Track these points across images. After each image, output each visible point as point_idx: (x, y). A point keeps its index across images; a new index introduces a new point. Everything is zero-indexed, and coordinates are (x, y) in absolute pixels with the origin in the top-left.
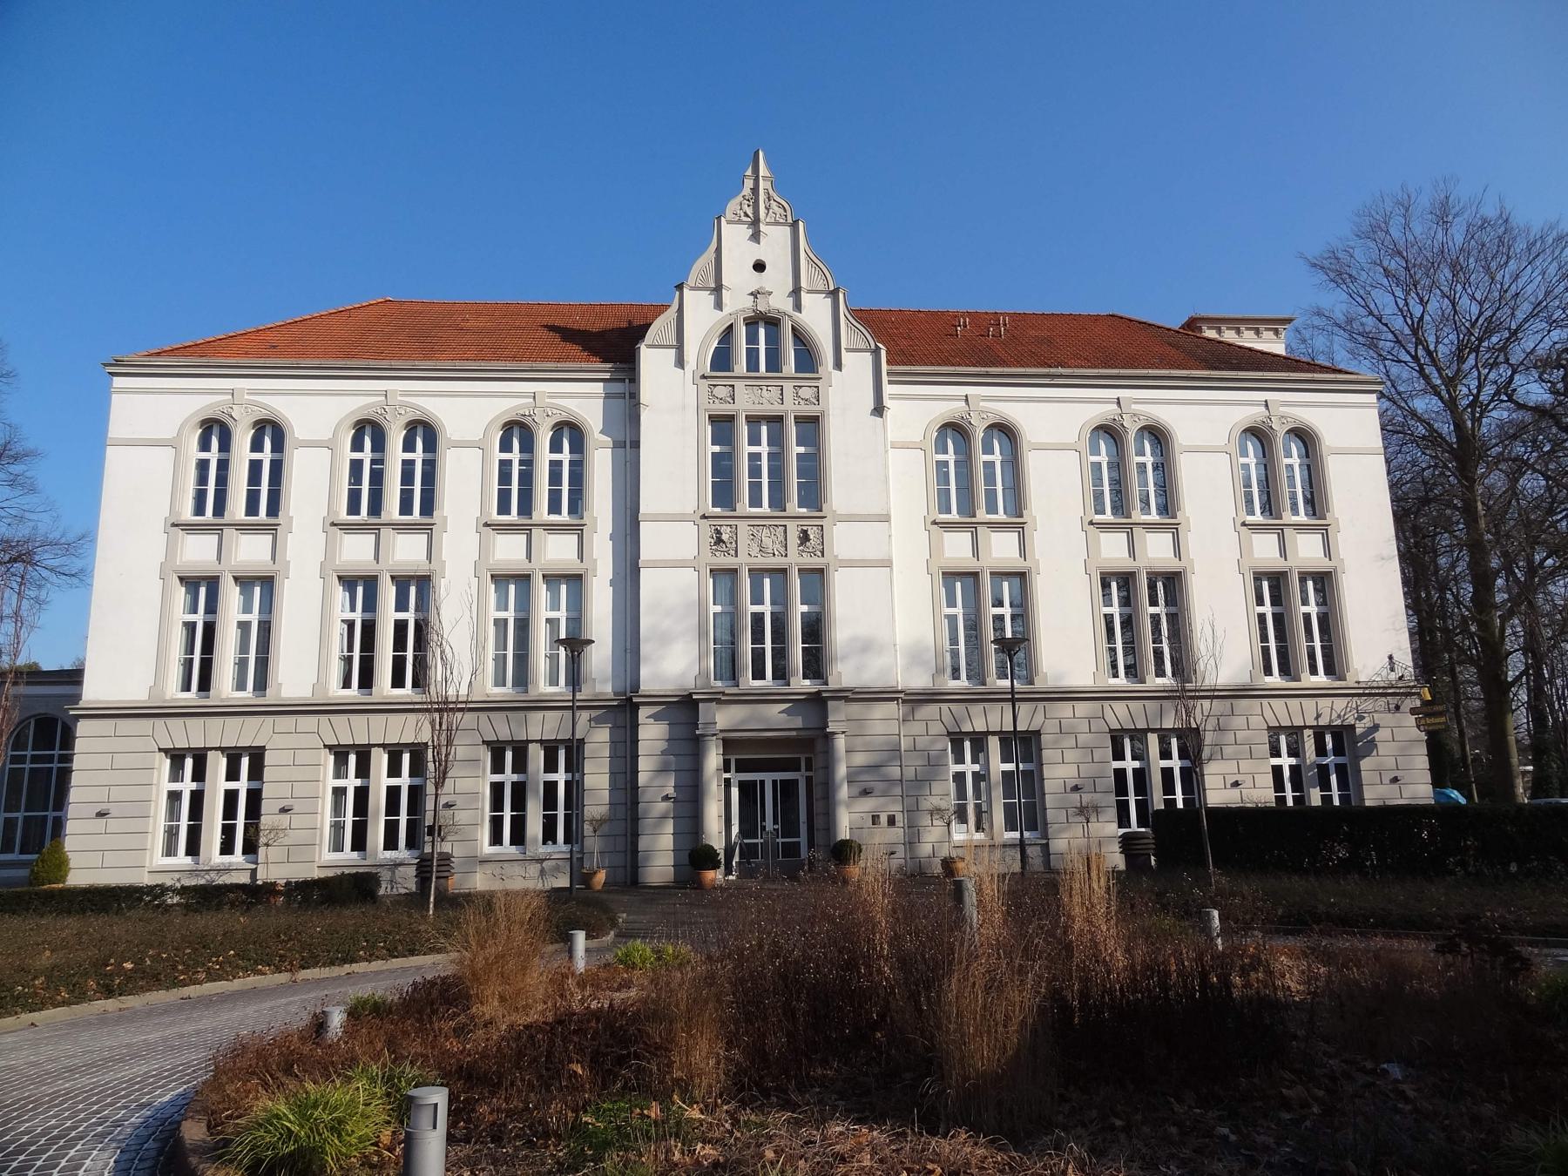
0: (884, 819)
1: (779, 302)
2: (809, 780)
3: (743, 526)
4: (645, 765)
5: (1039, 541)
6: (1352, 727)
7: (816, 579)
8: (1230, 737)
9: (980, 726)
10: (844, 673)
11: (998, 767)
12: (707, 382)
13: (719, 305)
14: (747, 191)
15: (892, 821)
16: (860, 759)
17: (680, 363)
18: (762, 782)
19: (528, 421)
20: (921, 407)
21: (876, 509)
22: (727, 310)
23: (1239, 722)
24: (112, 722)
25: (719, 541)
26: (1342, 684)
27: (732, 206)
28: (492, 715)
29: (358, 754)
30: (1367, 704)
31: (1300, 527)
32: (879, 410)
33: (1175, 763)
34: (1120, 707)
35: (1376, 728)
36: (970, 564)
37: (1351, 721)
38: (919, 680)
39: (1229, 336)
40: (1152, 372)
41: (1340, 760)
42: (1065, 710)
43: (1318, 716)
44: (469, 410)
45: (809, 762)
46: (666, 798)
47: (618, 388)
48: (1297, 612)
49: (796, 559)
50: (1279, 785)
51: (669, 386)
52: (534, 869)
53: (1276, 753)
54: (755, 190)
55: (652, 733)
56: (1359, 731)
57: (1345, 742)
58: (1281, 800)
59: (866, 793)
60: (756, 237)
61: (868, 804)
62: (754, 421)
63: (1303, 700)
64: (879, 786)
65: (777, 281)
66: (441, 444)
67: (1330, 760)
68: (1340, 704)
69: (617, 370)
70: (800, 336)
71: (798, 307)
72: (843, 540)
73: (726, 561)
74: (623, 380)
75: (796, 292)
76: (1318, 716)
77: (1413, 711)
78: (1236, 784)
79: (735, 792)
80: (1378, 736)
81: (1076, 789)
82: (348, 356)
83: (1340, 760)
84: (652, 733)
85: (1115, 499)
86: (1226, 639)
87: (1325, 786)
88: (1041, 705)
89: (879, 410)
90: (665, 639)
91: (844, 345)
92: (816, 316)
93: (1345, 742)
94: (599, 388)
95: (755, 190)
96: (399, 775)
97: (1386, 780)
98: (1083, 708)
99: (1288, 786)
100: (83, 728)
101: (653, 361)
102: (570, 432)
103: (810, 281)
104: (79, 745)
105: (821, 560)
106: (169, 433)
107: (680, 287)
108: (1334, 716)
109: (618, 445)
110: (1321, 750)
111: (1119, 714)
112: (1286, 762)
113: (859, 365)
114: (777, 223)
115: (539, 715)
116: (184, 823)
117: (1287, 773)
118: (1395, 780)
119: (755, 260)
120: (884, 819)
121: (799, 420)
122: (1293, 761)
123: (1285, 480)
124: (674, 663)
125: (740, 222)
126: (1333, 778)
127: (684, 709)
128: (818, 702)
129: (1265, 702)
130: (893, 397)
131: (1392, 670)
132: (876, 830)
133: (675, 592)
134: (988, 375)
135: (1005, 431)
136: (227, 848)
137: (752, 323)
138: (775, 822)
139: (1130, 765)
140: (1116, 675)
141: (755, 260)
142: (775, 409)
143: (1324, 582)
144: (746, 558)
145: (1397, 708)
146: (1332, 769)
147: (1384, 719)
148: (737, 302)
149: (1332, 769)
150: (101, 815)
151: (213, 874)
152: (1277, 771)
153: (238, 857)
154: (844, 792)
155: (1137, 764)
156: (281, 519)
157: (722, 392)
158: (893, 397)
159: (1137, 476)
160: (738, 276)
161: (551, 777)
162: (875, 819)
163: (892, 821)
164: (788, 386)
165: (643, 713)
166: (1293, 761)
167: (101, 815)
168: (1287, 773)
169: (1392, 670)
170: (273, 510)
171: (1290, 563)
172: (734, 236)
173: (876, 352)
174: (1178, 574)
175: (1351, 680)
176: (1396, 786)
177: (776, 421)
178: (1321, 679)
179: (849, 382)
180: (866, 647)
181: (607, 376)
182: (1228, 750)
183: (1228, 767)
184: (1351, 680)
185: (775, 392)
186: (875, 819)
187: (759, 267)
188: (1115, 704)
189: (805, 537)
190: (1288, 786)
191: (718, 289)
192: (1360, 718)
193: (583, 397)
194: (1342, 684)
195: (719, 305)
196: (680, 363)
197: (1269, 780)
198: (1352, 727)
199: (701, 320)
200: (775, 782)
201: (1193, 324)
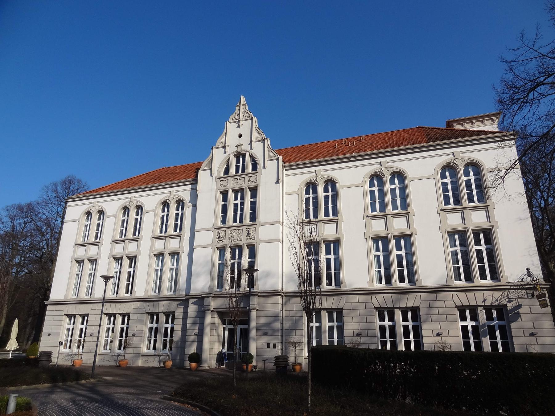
0: (272, 345)
1: (245, 147)
4: (189, 321)
5: (344, 226)
6: (506, 306)
7: (252, 249)
8: (435, 311)
10: (261, 285)
11: (326, 324)
13: (225, 153)
14: (237, 111)
16: (263, 320)
17: (211, 175)
19: (168, 201)
22: (228, 154)
23: (438, 304)
25: (219, 237)
26: (499, 284)
27: (232, 118)
30: (514, 294)
33: (410, 323)
34: (380, 297)
35: (520, 306)
37: (504, 302)
38: (292, 287)
39: (468, 127)
40: (395, 149)
41: (502, 323)
42: (354, 299)
43: (484, 301)
44: (151, 199)
46: (195, 334)
48: (476, 250)
49: (245, 241)
51: (207, 183)
52: (157, 359)
53: (463, 318)
56: (509, 308)
57: (504, 315)
58: (467, 345)
59: (265, 334)
61: (265, 339)
62: (235, 192)
63: (475, 292)
64: (270, 332)
65: (245, 141)
67: (495, 323)
68: (497, 294)
71: (251, 148)
72: (263, 233)
73: (221, 244)
76: (484, 301)
78: (438, 335)
79: (227, 332)
80: (521, 311)
81: (358, 335)
82: (127, 187)
83: (502, 323)
85: (378, 205)
86: (434, 264)
87: (493, 336)
88: (343, 297)
90: (198, 275)
92: (258, 150)
93: (504, 315)
95: (239, 110)
97: (527, 334)
98: (362, 298)
99: (471, 336)
100: (49, 308)
101: (203, 175)
102: (180, 203)
103: (256, 137)
107: (212, 148)
108: (494, 300)
110: (489, 317)
111: (378, 301)
112: (469, 323)
113: (271, 166)
114: (246, 120)
117: (470, 329)
118: (532, 334)
119: (240, 132)
120: (272, 345)
122: (474, 323)
123: (465, 188)
125: (234, 122)
126: (498, 333)
127: (201, 299)
128: (247, 297)
129: (454, 293)
130: (287, 175)
132: (268, 350)
133: (206, 256)
138: (240, 345)
139: (387, 324)
140: (381, 283)
141: (240, 132)
143: (488, 235)
146: (497, 327)
147: (525, 302)
148: (231, 149)
149: (497, 327)
152: (464, 328)
154: (253, 333)
155: (390, 324)
157: (224, 183)
158: (287, 175)
159: (389, 194)
161: (167, 325)
162: (269, 346)
163: (275, 346)
166: (474, 323)
168: (470, 329)
171: (467, 226)
172: (231, 129)
173: (278, 159)
174: (490, 230)
175: (503, 282)
176: (533, 338)
177: (242, 190)
178: (489, 281)
180: (268, 275)
181: (191, 182)
182: (434, 318)
183: (437, 326)
184: (503, 282)
186: (269, 346)
187: (240, 136)
188: (377, 296)
190: (471, 336)
191: (224, 147)
192: (510, 301)
194: (499, 284)
195: (225, 153)
196: (211, 175)
198: (506, 306)
199: (218, 157)
200: (241, 329)
201: (449, 124)
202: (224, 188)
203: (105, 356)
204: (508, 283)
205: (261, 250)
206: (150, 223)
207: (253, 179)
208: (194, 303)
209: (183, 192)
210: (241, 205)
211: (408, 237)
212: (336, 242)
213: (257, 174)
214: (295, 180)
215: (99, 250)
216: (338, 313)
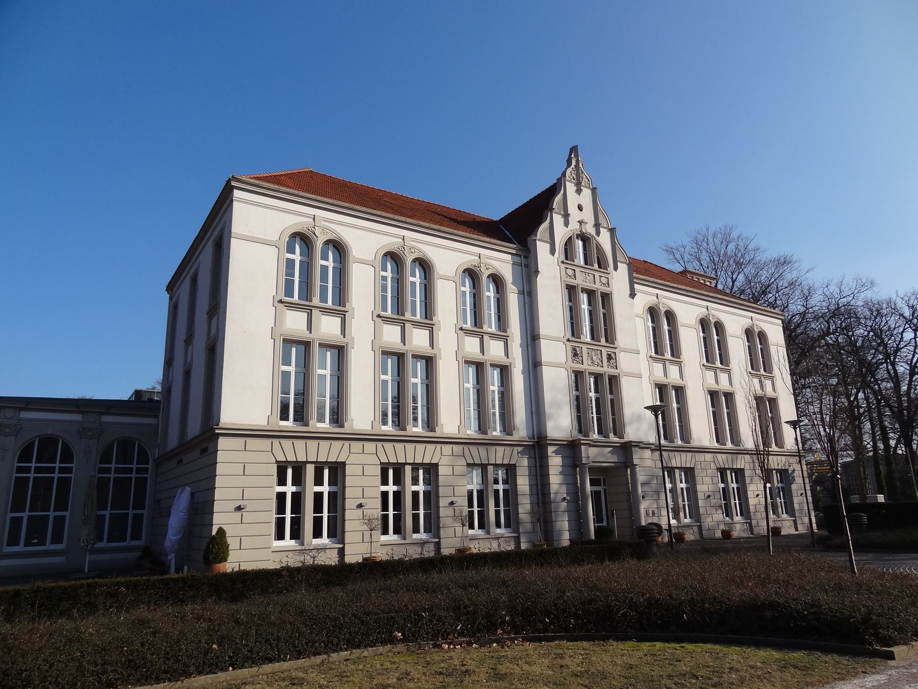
1: (590, 229)
2: (605, 490)
3: (584, 347)
6: (787, 470)
12: (563, 266)
13: (566, 224)
15: (653, 514)
17: (553, 252)
20: (647, 296)
24: (242, 440)
25: (575, 355)
28: (471, 447)
29: (394, 469)
32: (633, 295)
42: (700, 457)
46: (564, 499)
47: (518, 259)
49: (606, 369)
51: (548, 262)
54: (577, 166)
55: (555, 462)
60: (579, 191)
65: (588, 215)
68: (784, 458)
69: (520, 250)
70: (599, 249)
71: (598, 233)
72: (625, 362)
73: (579, 367)
74: (520, 256)
75: (597, 226)
81: (709, 496)
84: (555, 462)
89: (633, 295)
94: (509, 257)
96: (322, 484)
98: (709, 457)
102: (496, 279)
104: (220, 456)
105: (615, 371)
106: (274, 237)
109: (521, 293)
113: (623, 268)
115: (494, 448)
116: (288, 516)
124: (560, 423)
127: (571, 448)
136: (317, 534)
137: (578, 236)
142: (591, 286)
144: (586, 366)
148: (574, 226)
150: (239, 508)
151: (314, 553)
153: (325, 540)
156: (348, 307)
160: (572, 209)
163: (653, 514)
164: (597, 275)
165: (551, 450)
167: (239, 508)
179: (619, 279)
181: (514, 252)
185: (591, 277)
189: (609, 357)
191: (566, 216)
193: (500, 260)
195: (566, 224)
198: (787, 470)
203: (395, 548)
208: (556, 452)
210: (594, 317)
213: (609, 276)
216: (689, 473)
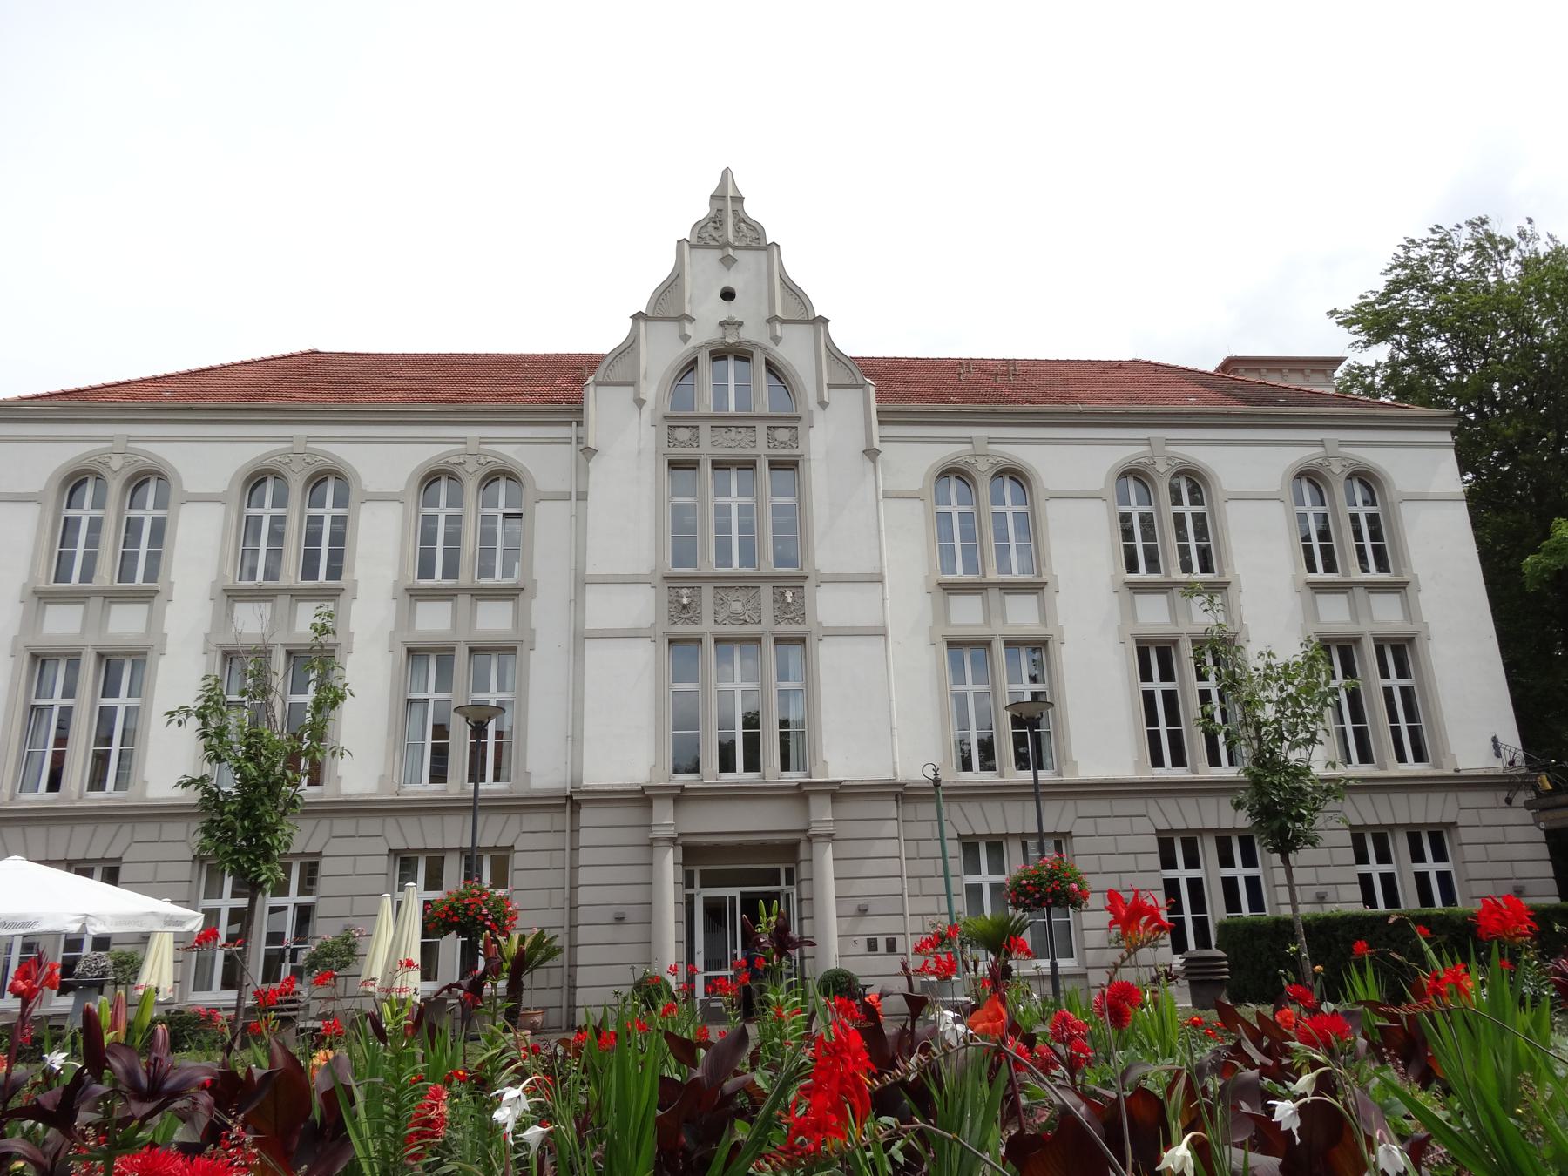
1: (753, 333)
9: (998, 828)
17: (640, 403)
18: (733, 899)
21: (866, 567)
31: (1373, 587)
36: (981, 632)
45: (790, 872)
50: (1369, 899)
66: (354, 497)
77: (1528, 805)
89: (871, 453)
91: (826, 381)
121: (775, 465)
131: (1498, 755)
134: (994, 413)
135: (1015, 475)
137: (718, 355)
145: (1509, 801)
148: (704, 331)
157: (683, 434)
158: (883, 440)
169: (1498, 755)
170: (151, 574)
197: (1356, 892)
202: (681, 452)
204: (1457, 771)
205: (827, 655)
206: (380, 545)
207: (783, 435)
209: (534, 452)
211: (1038, 646)
212: (1038, 646)
214: (916, 457)
215: (154, 621)
